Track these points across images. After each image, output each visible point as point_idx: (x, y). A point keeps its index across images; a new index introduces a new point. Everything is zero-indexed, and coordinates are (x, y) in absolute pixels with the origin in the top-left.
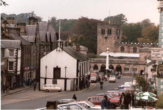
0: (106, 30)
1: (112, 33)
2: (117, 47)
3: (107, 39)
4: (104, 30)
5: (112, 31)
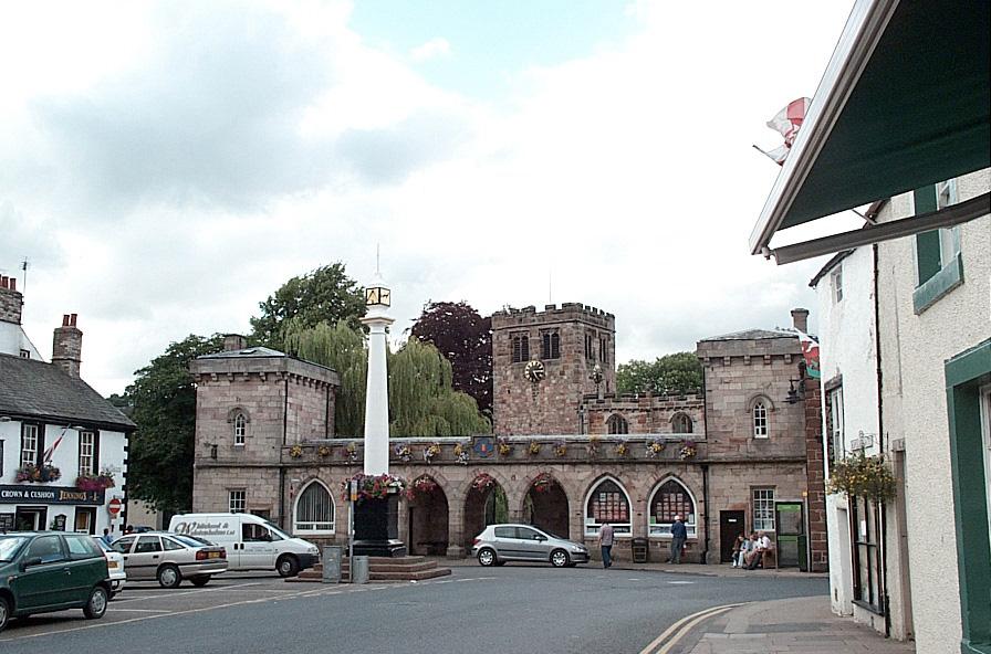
0: (534, 337)
5: (562, 339)
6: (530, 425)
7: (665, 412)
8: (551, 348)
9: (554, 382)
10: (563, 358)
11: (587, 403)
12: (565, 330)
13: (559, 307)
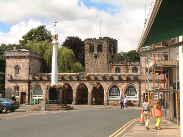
0: (96, 46)
1: (103, 49)
2: (111, 69)
3: (97, 59)
4: (93, 46)
5: (103, 47)
6: (94, 69)
7: (130, 66)
8: (100, 49)
10: (103, 52)
12: (104, 44)
13: (103, 38)
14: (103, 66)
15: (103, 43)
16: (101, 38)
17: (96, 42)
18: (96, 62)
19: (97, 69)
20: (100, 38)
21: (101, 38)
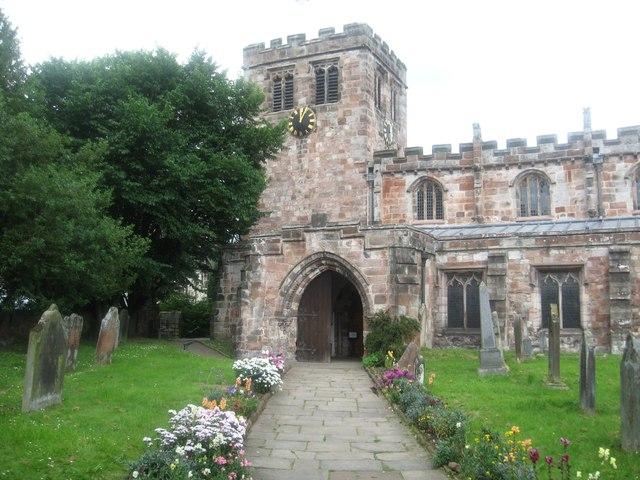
0: (304, 74)
2: (386, 190)
3: (309, 141)
4: (290, 77)
5: (344, 74)
6: (293, 198)
7: (503, 171)
8: (327, 88)
9: (329, 134)
11: (379, 162)
14: (340, 178)
15: (340, 55)
16: (333, 30)
17: (302, 51)
18: (300, 156)
19: (306, 197)
20: (328, 35)
21: (333, 30)
